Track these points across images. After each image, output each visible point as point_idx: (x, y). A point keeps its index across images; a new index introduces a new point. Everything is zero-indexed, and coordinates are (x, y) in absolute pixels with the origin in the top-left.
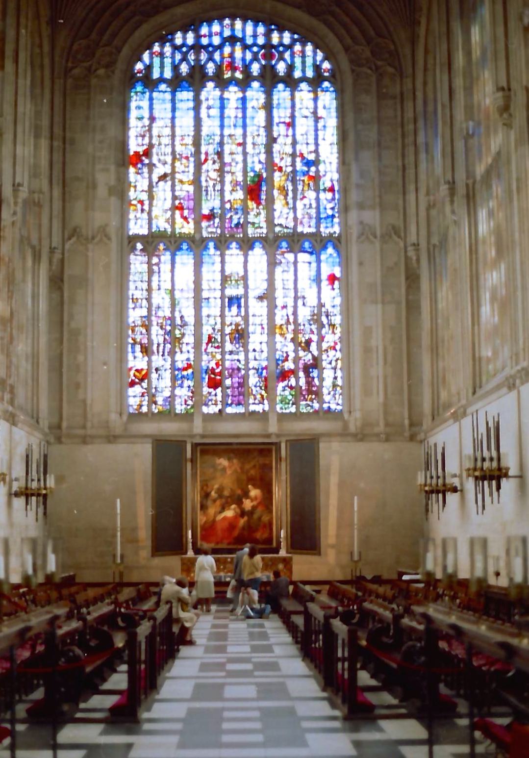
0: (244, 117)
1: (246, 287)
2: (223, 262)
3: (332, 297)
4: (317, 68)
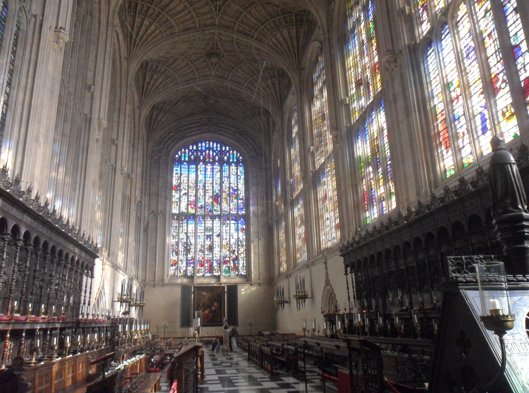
0: (213, 174)
1: (213, 232)
2: (205, 223)
3: (242, 236)
4: (238, 158)
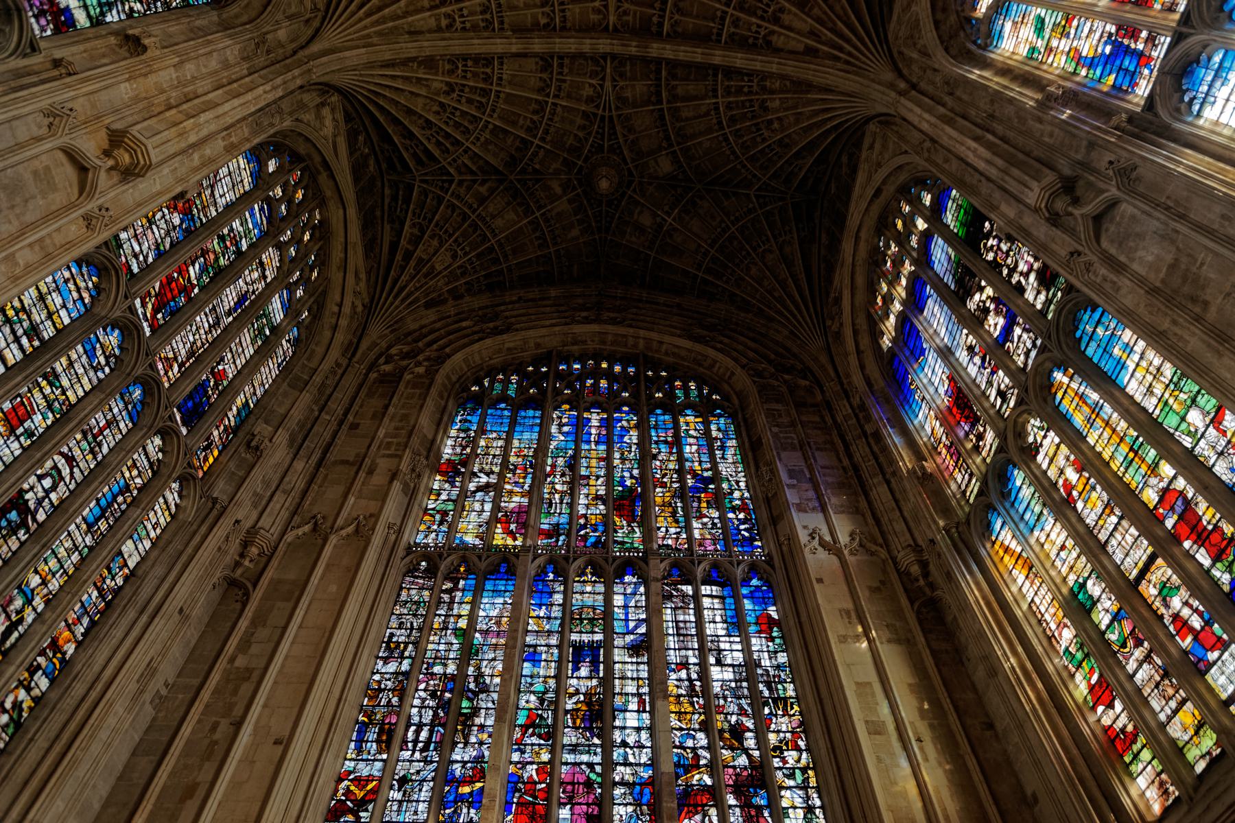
1: (609, 631)
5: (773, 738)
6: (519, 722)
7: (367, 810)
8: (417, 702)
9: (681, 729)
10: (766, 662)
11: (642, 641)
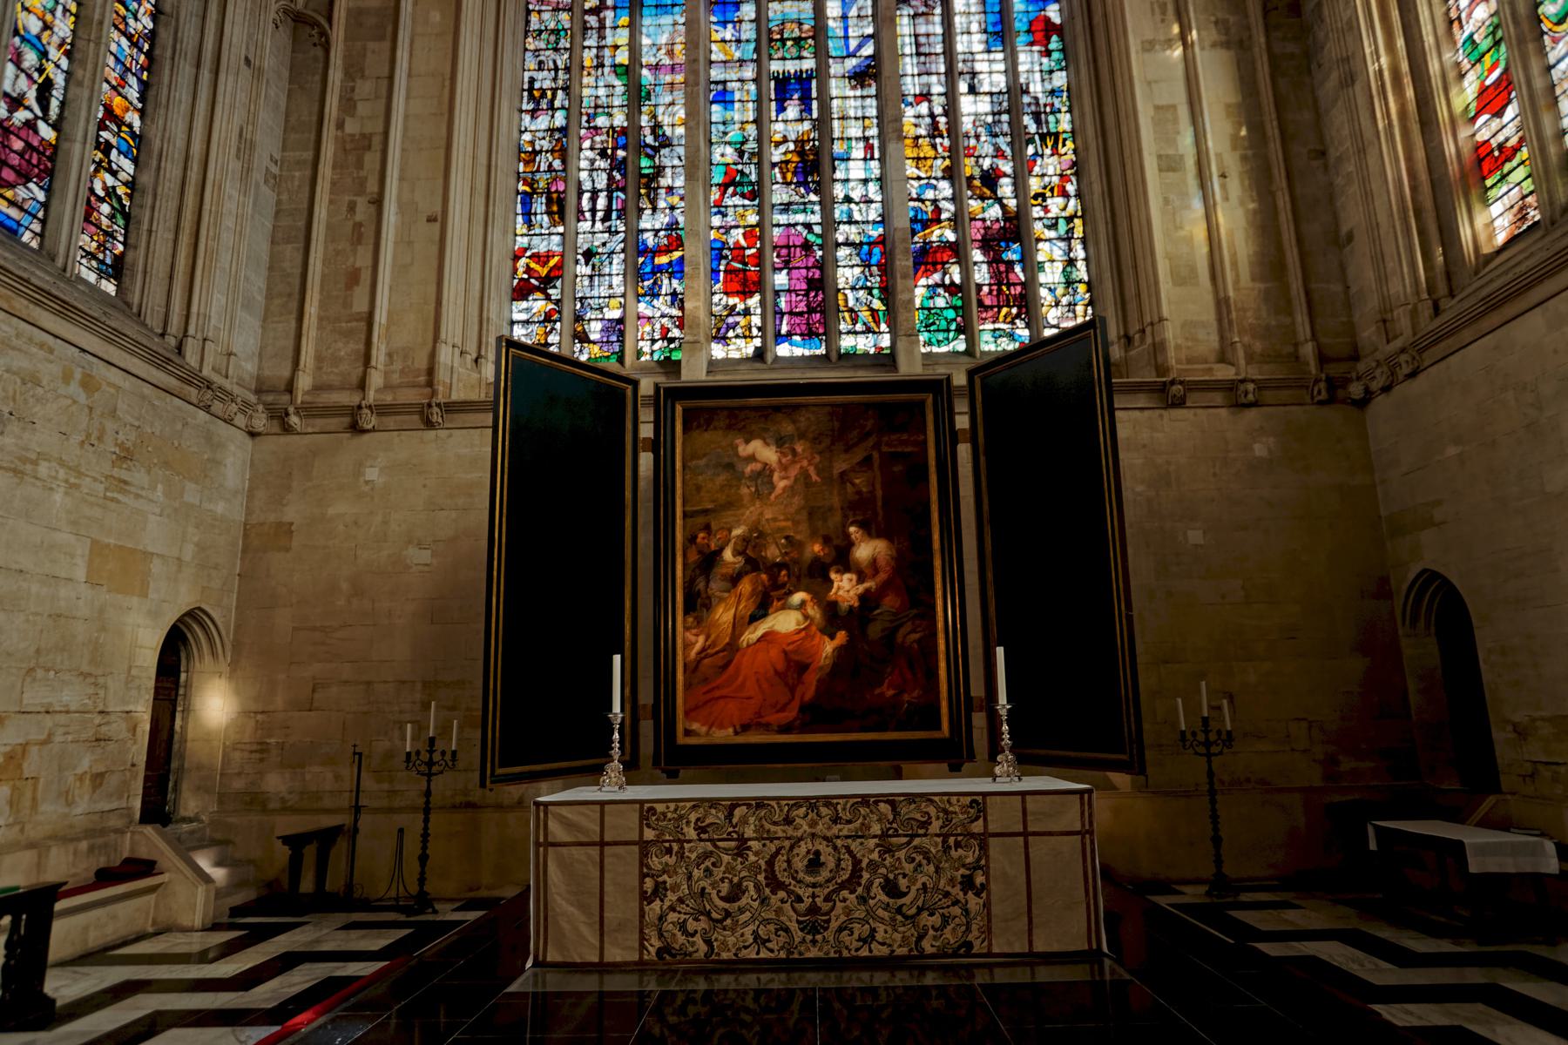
1: (822, 54)
5: (1035, 185)
6: (715, 181)
7: (555, 287)
8: (584, 164)
9: (919, 178)
10: (1036, 88)
11: (869, 66)
